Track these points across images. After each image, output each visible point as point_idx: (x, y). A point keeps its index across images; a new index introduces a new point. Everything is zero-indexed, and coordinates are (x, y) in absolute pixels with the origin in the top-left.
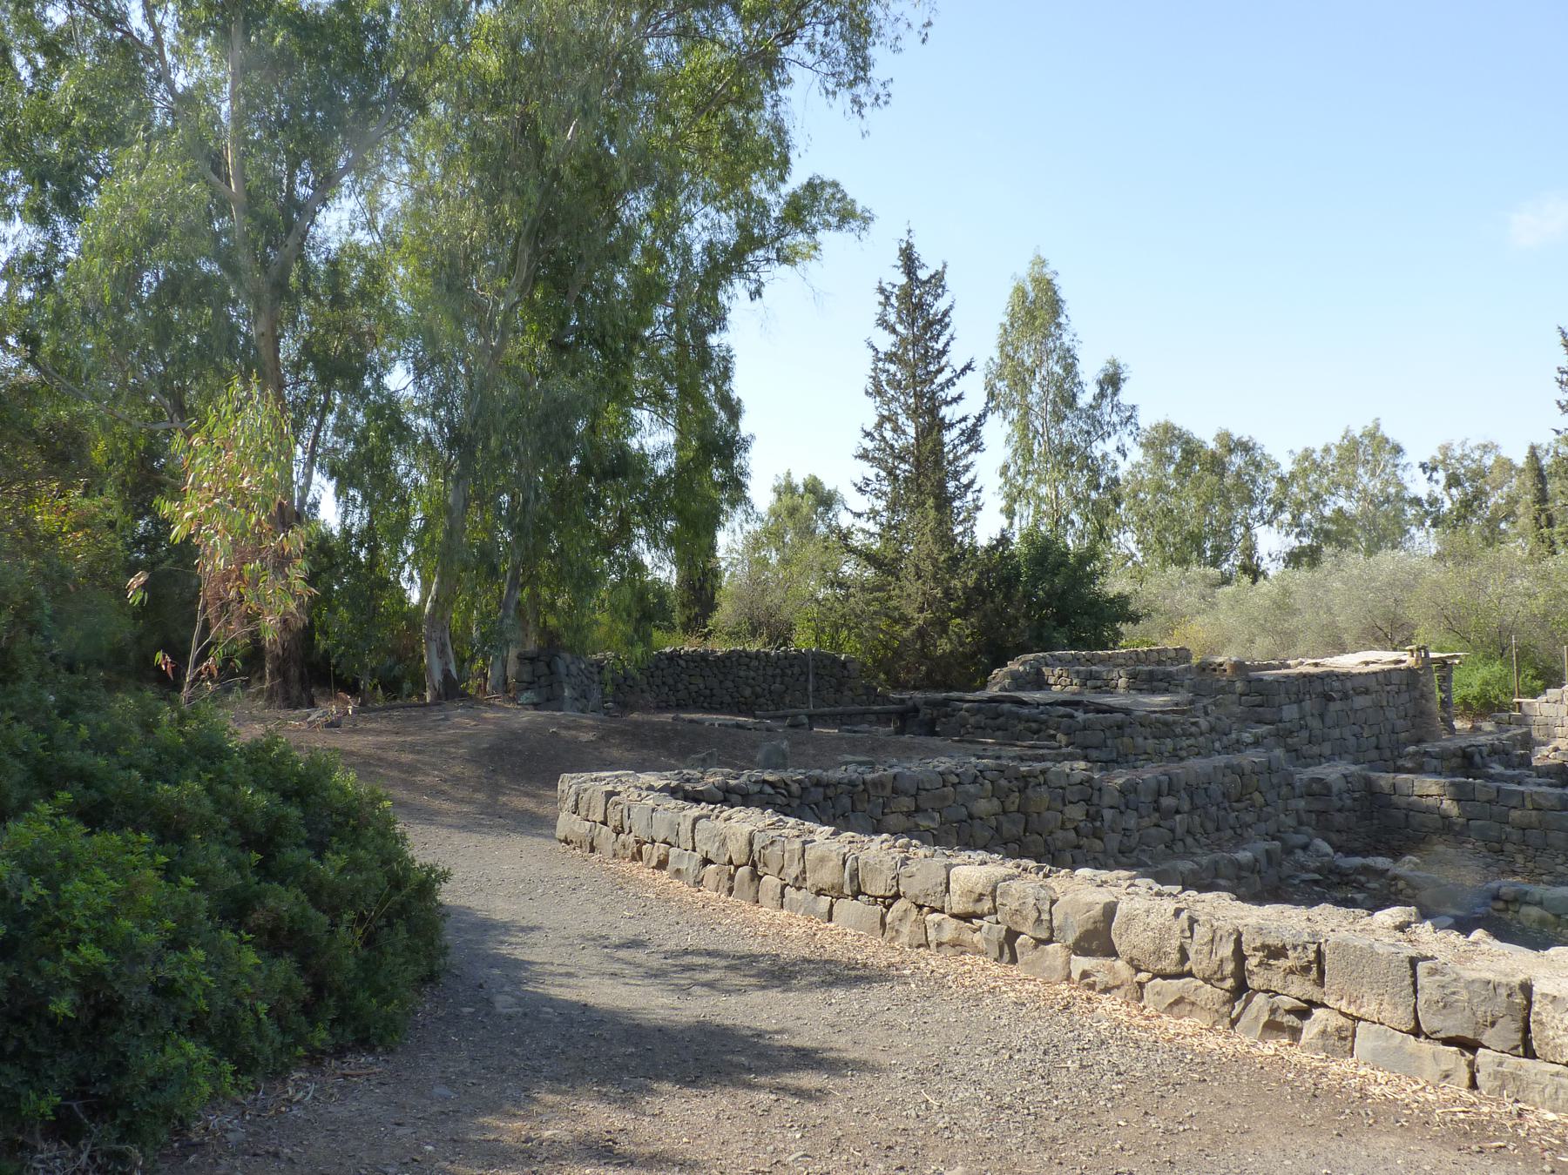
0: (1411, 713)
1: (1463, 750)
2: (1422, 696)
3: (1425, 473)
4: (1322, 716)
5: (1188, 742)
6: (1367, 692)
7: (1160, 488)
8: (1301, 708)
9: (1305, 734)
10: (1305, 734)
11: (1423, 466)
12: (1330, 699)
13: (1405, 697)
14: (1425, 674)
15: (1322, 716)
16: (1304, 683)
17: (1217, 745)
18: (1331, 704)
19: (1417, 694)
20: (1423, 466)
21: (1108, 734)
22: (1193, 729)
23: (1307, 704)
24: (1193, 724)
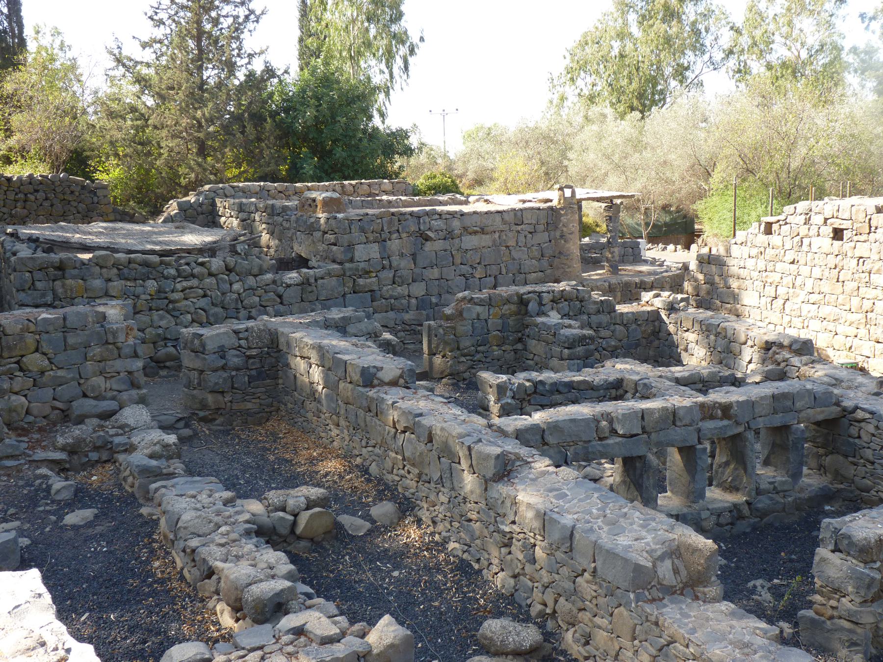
0: (548, 252)
1: (520, 297)
2: (562, 236)
3: (863, 22)
4: (414, 256)
5: (185, 284)
6: (483, 231)
7: (622, 35)
8: (383, 249)
9: (388, 275)
10: (388, 275)
11: (862, 16)
12: (427, 239)
13: (542, 237)
14: (566, 214)
15: (414, 256)
16: (390, 222)
17: (236, 287)
18: (428, 244)
19: (558, 234)
20: (862, 16)
21: (38, 275)
22: (198, 270)
23: (394, 245)
24: (202, 264)
